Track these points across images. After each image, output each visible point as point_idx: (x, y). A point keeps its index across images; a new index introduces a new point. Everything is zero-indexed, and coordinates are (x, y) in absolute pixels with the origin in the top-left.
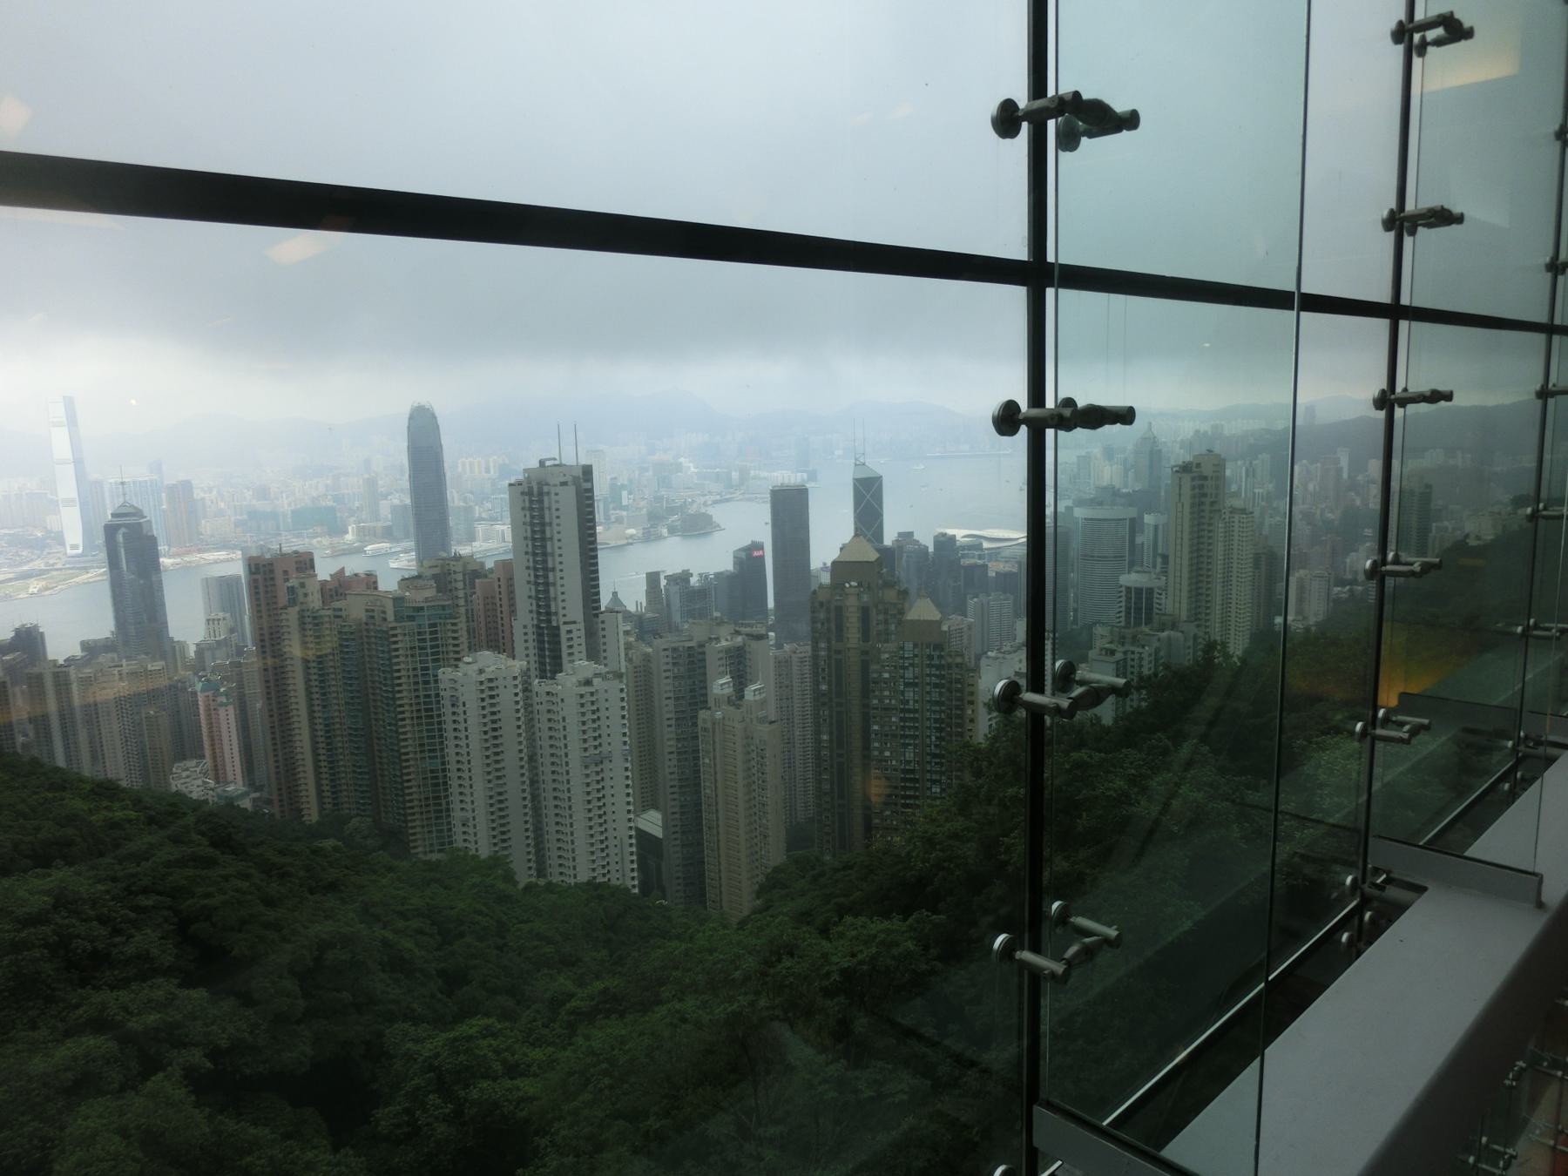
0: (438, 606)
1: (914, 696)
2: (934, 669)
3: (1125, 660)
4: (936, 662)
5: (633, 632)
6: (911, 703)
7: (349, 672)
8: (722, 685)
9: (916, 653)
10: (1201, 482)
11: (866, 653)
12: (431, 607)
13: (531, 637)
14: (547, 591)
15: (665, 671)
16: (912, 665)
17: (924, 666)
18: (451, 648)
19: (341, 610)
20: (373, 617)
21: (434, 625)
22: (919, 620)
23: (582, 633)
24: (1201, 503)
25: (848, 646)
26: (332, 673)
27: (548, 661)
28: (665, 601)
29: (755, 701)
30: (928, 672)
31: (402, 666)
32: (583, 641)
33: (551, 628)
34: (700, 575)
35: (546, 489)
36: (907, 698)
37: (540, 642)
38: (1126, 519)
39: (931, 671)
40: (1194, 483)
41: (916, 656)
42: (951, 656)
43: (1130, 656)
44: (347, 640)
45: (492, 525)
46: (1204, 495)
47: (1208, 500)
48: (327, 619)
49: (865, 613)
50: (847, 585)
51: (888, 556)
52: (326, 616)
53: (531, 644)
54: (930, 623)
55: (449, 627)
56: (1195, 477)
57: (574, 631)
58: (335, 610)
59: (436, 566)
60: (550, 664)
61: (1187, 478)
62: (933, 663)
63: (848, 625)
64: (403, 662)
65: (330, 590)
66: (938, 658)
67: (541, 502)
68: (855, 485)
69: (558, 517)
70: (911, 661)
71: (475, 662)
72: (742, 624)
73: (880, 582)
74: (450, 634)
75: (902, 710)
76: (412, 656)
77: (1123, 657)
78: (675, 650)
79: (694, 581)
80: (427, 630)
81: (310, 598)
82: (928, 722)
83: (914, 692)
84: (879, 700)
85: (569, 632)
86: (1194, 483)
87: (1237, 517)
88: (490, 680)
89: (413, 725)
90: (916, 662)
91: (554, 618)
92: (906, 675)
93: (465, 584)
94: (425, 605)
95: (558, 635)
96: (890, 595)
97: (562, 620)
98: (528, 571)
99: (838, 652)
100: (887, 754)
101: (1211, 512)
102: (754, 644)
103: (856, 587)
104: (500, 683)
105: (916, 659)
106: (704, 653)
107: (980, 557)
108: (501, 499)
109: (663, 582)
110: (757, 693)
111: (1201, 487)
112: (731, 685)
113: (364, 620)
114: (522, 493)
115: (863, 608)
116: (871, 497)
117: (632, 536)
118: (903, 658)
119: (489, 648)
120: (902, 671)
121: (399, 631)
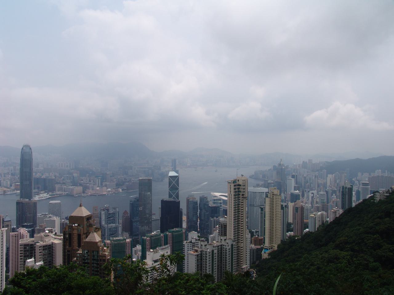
2: (95, 261)
3: (201, 254)
9: (89, 254)
10: (238, 187)
16: (87, 259)
17: (92, 260)
24: (240, 195)
30: (93, 262)
38: (264, 192)
39: (94, 262)
40: (235, 187)
43: (203, 253)
46: (240, 192)
47: (241, 194)
49: (79, 236)
50: (74, 225)
56: (236, 185)
61: (233, 185)
62: (95, 258)
68: (169, 179)
70: (87, 258)
77: (200, 253)
86: (235, 187)
87: (275, 196)
99: (68, 251)
101: (242, 198)
106: (35, 247)
107: (221, 203)
108: (67, 177)
111: (239, 188)
115: (78, 234)
117: (109, 191)
118: (84, 256)
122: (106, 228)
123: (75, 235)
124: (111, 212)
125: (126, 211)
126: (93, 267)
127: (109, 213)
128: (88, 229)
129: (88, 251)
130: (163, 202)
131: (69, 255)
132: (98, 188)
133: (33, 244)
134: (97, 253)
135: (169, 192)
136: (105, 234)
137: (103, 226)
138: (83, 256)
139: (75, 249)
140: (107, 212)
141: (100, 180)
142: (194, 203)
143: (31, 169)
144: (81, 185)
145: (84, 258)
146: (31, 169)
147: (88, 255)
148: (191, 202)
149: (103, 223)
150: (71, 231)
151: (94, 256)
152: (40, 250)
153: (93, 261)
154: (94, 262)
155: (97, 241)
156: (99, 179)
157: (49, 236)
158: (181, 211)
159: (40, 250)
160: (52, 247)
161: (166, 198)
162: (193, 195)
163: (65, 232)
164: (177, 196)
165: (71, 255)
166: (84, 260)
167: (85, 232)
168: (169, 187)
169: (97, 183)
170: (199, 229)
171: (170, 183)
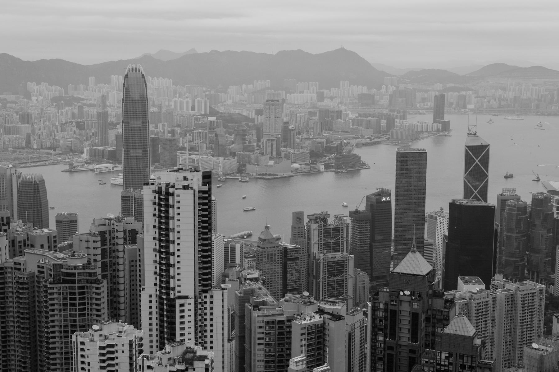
0: (86, 273)
5: (260, 278)
7: (22, 314)
8: (296, 363)
9: (451, 361)
11: (412, 351)
12: (81, 273)
13: (154, 304)
14: (168, 271)
15: (259, 339)
18: (94, 307)
19: (20, 264)
20: (43, 272)
21: (83, 288)
22: (455, 335)
23: (192, 307)
25: (400, 343)
26: (11, 311)
27: (165, 325)
28: (306, 235)
31: (56, 318)
32: (192, 313)
33: (169, 299)
34: (336, 217)
35: (171, 190)
41: (450, 364)
42: (481, 368)
44: (23, 289)
45: (190, 154)
48: (10, 270)
49: (415, 316)
50: (401, 293)
51: (490, 210)
52: (9, 267)
53: (154, 310)
54: (465, 338)
55: (94, 290)
58: (15, 263)
59: (105, 225)
60: (167, 327)
63: (401, 326)
64: (57, 315)
65: (20, 242)
66: (469, 368)
67: (167, 200)
68: (467, 152)
69: (178, 214)
70: (446, 368)
71: (101, 330)
72: (328, 302)
73: (430, 292)
74: (94, 296)
76: (64, 310)
79: (330, 221)
80: (77, 291)
85: (182, 305)
88: (112, 346)
89: (62, 364)
90: (450, 369)
91: (172, 292)
93: (125, 239)
94: (76, 271)
95: (174, 306)
96: (438, 304)
97: (177, 294)
98: (155, 253)
99: (390, 348)
102: (332, 325)
103: (408, 296)
104: (119, 348)
105: (451, 366)
106: (290, 327)
108: (200, 133)
109: (306, 220)
112: (305, 362)
113: (36, 272)
114: (154, 191)
115: (413, 313)
116: (478, 161)
117: (296, 170)
118: (439, 364)
119: (114, 316)
121: (55, 290)
122: (322, 261)
123: (403, 314)
124: (331, 227)
127: (328, 227)
128: (430, 303)
129: (449, 354)
131: (390, 356)
132: (272, 162)
133: (283, 321)
134: (472, 361)
136: (320, 274)
137: (314, 257)
138: (438, 364)
139: (406, 344)
140: (324, 226)
141: (274, 143)
142: (519, 209)
143: (145, 123)
145: (440, 368)
147: (449, 362)
148: (509, 206)
149: (315, 249)
150: (395, 305)
152: (302, 334)
155: (471, 334)
156: (272, 140)
158: (496, 230)
159: (302, 334)
160: (325, 329)
161: (459, 196)
162: (514, 190)
163: (376, 305)
164: (484, 194)
165: (395, 356)
168: (465, 173)
170: (526, 272)
171: (469, 161)
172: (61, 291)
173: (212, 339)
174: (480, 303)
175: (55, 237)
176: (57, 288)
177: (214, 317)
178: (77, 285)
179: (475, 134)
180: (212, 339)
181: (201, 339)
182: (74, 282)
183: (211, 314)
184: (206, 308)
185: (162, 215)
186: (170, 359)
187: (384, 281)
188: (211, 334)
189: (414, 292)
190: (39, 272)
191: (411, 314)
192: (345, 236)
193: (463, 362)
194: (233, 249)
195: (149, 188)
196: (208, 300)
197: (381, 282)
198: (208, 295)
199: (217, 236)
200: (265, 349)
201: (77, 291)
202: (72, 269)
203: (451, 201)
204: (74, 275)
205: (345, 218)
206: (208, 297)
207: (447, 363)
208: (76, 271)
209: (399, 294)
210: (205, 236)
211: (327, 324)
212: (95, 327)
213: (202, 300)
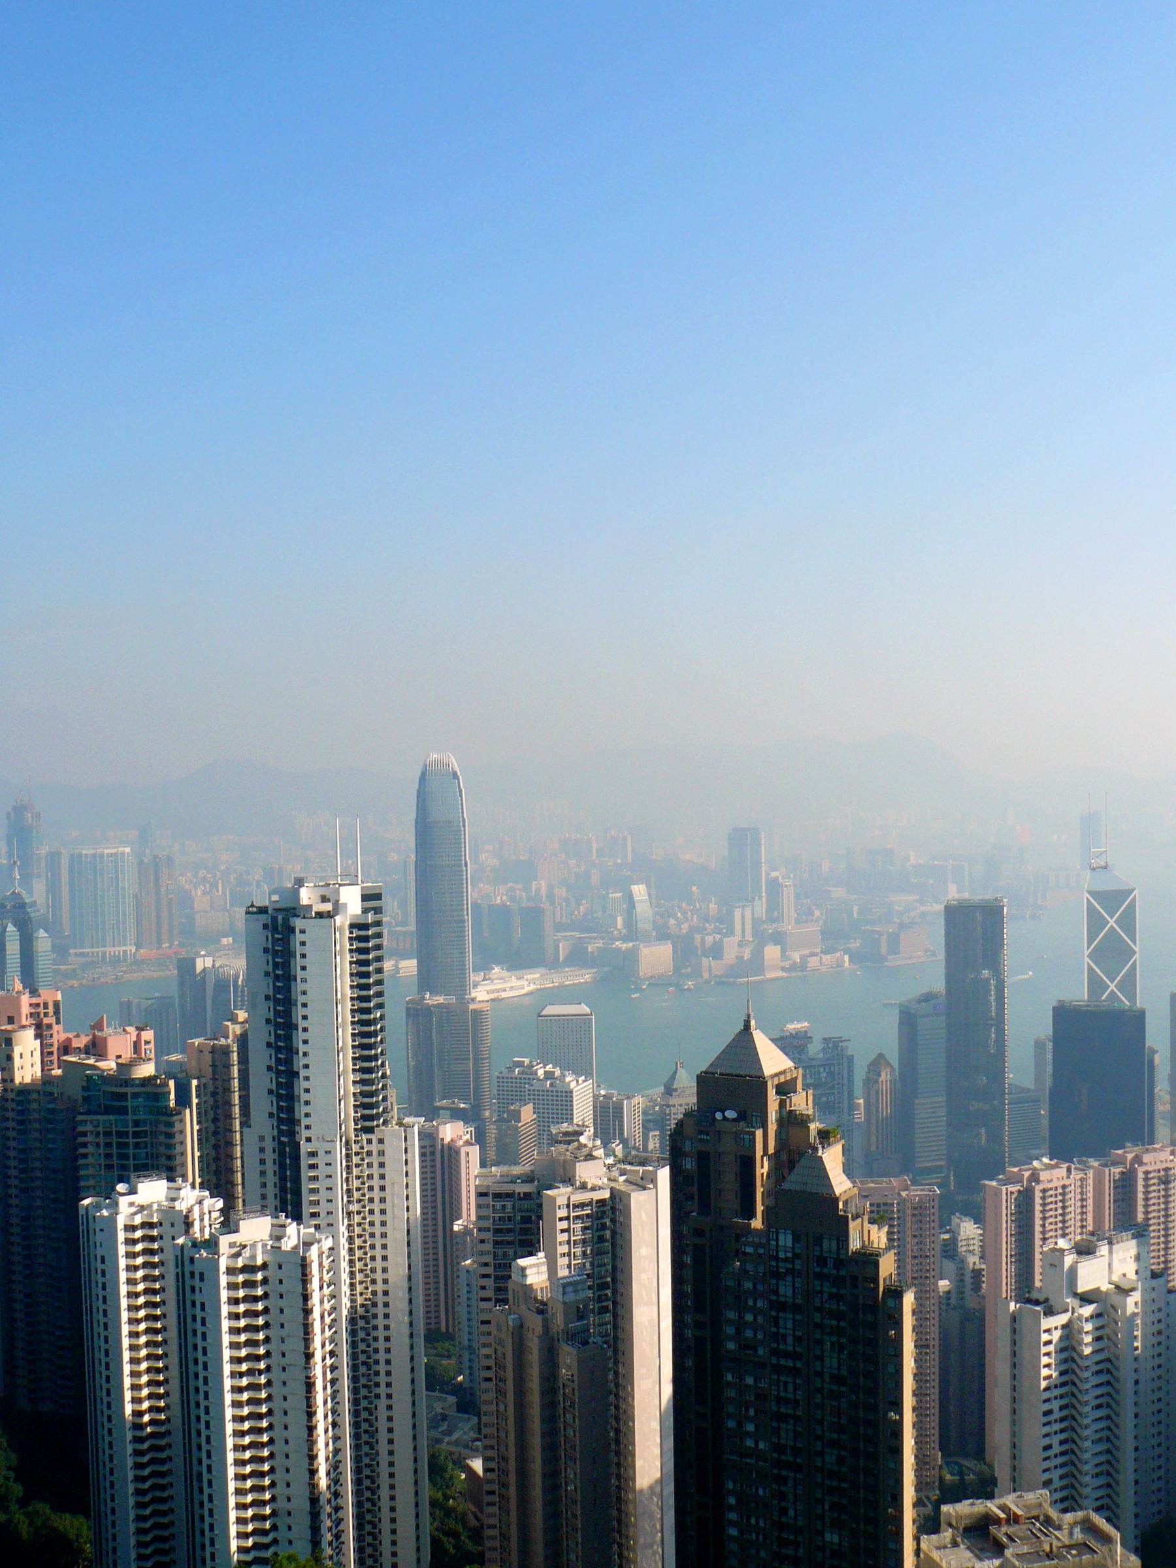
0: (147, 1093)
1: (794, 1329)
2: (827, 1284)
4: (830, 1270)
6: (790, 1340)
13: (270, 1156)
16: (791, 1272)
22: (804, 1192)
27: (289, 1196)
29: (564, 1303)
30: (818, 1288)
34: (826, 1040)
36: (782, 1331)
37: (282, 1166)
39: (822, 1286)
50: (719, 1116)
53: (270, 1168)
55: (163, 1128)
57: (321, 1153)
62: (825, 1271)
70: (790, 1266)
75: (775, 1353)
78: (498, 1196)
80: (131, 1129)
81: (17, 1062)
82: (818, 1380)
83: (794, 1320)
84: (738, 1330)
85: (313, 1154)
88: (151, 1225)
90: (797, 1267)
92: (782, 1290)
94: (128, 1090)
100: (750, 1427)
103: (734, 1120)
105: (798, 1262)
110: (570, 1289)
115: (741, 1157)
117: (793, 968)
118: (777, 1258)
120: (773, 1281)
125: (881, 1055)
126: (819, 1310)
128: (784, 1137)
130: (1064, 1015)
134: (838, 1250)
135: (1090, 969)
138: (771, 1258)
144: (663, 935)
145: (777, 1267)
146: (460, 865)
151: (822, 1261)
153: (817, 1283)
154: (822, 1286)
157: (595, 1158)
160: (613, 1209)
161: (1079, 993)
166: (776, 1274)
167: (771, 1150)
169: (738, 927)
171: (1095, 922)
172: (100, 1129)
173: (384, 1230)
174: (1051, 1189)
175: (147, 1043)
176: (91, 1122)
177: (387, 1183)
178: (130, 1117)
179: (1105, 868)
180: (384, 1230)
181: (360, 1228)
182: (123, 1111)
183: (382, 1177)
184: (370, 1165)
185: (279, 972)
186: (232, 1245)
187: (938, 1178)
188: (383, 1218)
189: (745, 1111)
190: (84, 1098)
191: (738, 1160)
192: (846, 1081)
193: (822, 1251)
194: (619, 1109)
195: (258, 920)
196: (374, 1148)
197: (933, 1179)
198: (374, 1137)
199: (580, 1082)
200: (494, 1252)
201: (131, 1129)
202: (121, 1086)
203: (1055, 1004)
204: (123, 1097)
205: (844, 1044)
206: (375, 1141)
207: (789, 1255)
208: (128, 1090)
209: (714, 1118)
210: (365, 1017)
211: (617, 1200)
212: (121, 1187)
213: (362, 1148)
